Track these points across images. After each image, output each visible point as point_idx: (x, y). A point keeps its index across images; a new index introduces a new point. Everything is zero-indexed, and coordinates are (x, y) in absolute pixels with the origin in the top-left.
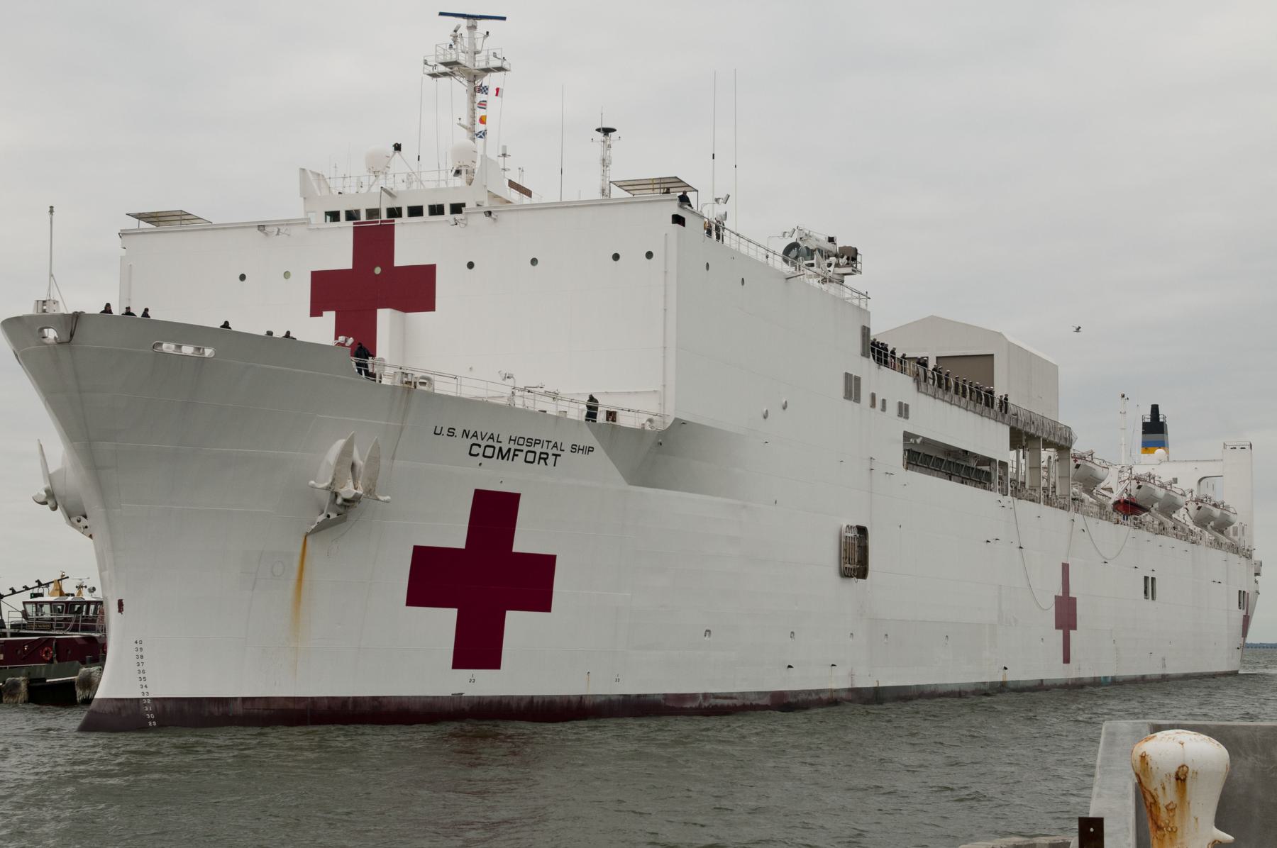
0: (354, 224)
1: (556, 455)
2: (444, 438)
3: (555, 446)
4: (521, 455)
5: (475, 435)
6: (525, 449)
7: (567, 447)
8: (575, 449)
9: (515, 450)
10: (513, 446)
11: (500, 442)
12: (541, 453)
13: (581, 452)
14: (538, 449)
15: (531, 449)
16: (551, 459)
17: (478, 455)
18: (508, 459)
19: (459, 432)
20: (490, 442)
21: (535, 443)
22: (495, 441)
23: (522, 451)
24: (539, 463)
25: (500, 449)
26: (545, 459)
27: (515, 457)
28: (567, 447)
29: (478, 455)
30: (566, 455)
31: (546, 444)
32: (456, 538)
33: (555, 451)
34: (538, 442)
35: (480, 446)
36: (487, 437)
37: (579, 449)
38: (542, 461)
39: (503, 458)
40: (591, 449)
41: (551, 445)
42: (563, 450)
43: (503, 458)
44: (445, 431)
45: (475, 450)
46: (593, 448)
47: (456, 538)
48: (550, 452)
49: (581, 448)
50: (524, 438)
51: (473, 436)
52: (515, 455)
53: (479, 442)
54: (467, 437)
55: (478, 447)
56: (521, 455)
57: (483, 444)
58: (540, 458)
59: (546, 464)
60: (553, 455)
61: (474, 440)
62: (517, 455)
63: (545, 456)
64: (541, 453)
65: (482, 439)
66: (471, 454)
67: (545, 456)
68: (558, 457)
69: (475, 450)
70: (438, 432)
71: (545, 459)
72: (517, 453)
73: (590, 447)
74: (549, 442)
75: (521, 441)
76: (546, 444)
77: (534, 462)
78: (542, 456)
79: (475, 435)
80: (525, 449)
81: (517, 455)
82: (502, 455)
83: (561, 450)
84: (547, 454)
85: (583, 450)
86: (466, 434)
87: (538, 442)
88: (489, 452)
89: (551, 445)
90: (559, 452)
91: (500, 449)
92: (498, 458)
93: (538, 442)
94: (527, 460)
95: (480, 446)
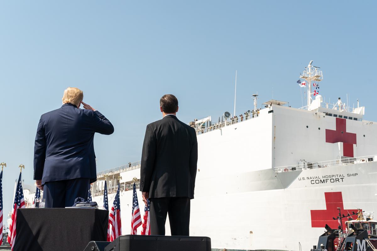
1: (342, 178)
2: (302, 181)
3: (340, 176)
4: (329, 181)
5: (311, 178)
7: (345, 175)
8: (348, 175)
12: (336, 179)
14: (334, 178)
15: (331, 178)
16: (340, 180)
19: (306, 178)
20: (317, 179)
25: (321, 180)
26: (338, 180)
28: (345, 175)
31: (336, 176)
33: (341, 177)
35: (314, 181)
36: (315, 178)
39: (323, 183)
41: (339, 176)
43: (323, 183)
44: (302, 179)
45: (313, 182)
48: (338, 178)
52: (326, 181)
53: (313, 180)
56: (329, 181)
57: (315, 180)
58: (336, 180)
61: (311, 180)
64: (336, 179)
67: (338, 179)
68: (343, 179)
69: (313, 182)
70: (300, 179)
72: (327, 180)
75: (327, 177)
77: (334, 182)
78: (336, 180)
79: (311, 178)
80: (330, 179)
86: (308, 178)
87: (333, 176)
88: (317, 182)
89: (339, 176)
90: (343, 177)
91: (321, 180)
95: (314, 181)
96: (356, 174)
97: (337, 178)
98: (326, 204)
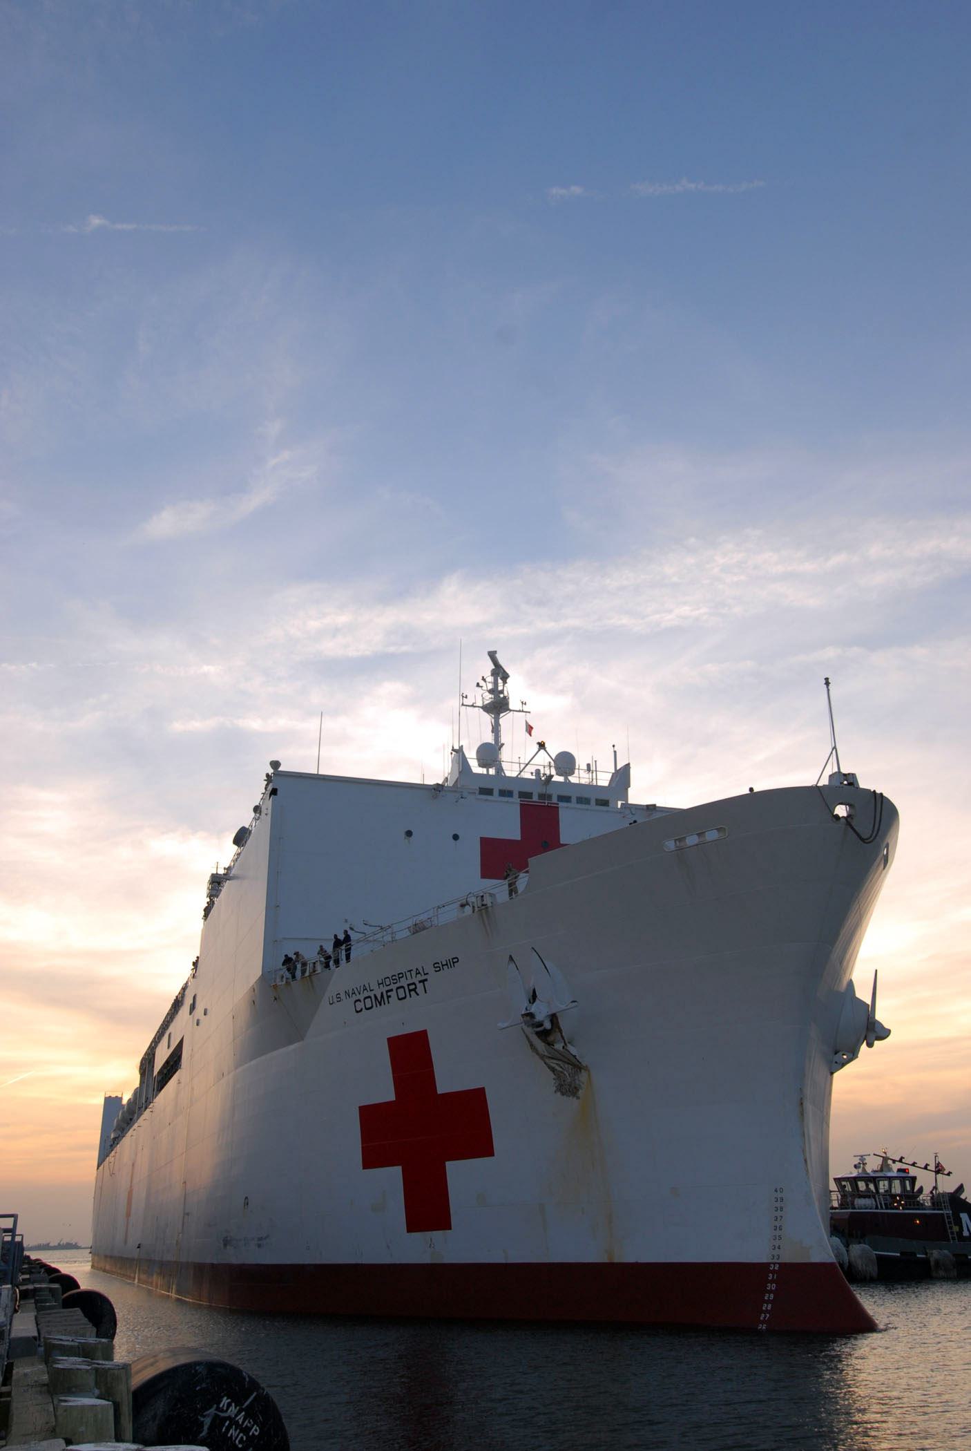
0: (521, 801)
1: (423, 981)
6: (394, 987)
7: (430, 969)
8: (438, 967)
9: (387, 992)
10: (384, 989)
11: (373, 990)
13: (445, 967)
14: (404, 982)
16: (420, 987)
17: (361, 1010)
18: (385, 1004)
19: (343, 996)
20: (366, 994)
21: (399, 978)
22: (368, 989)
23: (392, 990)
24: (411, 997)
27: (389, 999)
28: (430, 969)
29: (361, 1010)
30: (433, 978)
31: (408, 974)
32: (384, 1091)
34: (401, 975)
35: (359, 1000)
36: (362, 989)
37: (443, 965)
38: (413, 993)
39: (380, 1005)
40: (454, 960)
41: (414, 973)
42: (427, 974)
43: (380, 1005)
44: (335, 1000)
45: (360, 1006)
46: (457, 958)
47: (384, 1091)
48: (416, 980)
49: (444, 963)
50: (388, 978)
51: (353, 994)
53: (358, 997)
54: (349, 995)
55: (358, 1003)
56: (393, 994)
57: (361, 997)
58: (410, 991)
59: (418, 995)
60: (420, 982)
62: (390, 996)
63: (413, 987)
64: (409, 985)
65: (360, 994)
66: (357, 1012)
67: (413, 987)
69: (360, 1006)
71: (414, 990)
72: (389, 994)
73: (453, 959)
74: (410, 971)
76: (408, 974)
80: (394, 987)
81: (390, 996)
82: (380, 1000)
83: (425, 974)
84: (414, 984)
85: (447, 964)
87: (401, 976)
90: (424, 977)
92: (377, 1006)
93: (401, 975)
94: (400, 997)
95: (359, 1000)
96: (455, 960)
97: (410, 981)
98: (394, 1077)
